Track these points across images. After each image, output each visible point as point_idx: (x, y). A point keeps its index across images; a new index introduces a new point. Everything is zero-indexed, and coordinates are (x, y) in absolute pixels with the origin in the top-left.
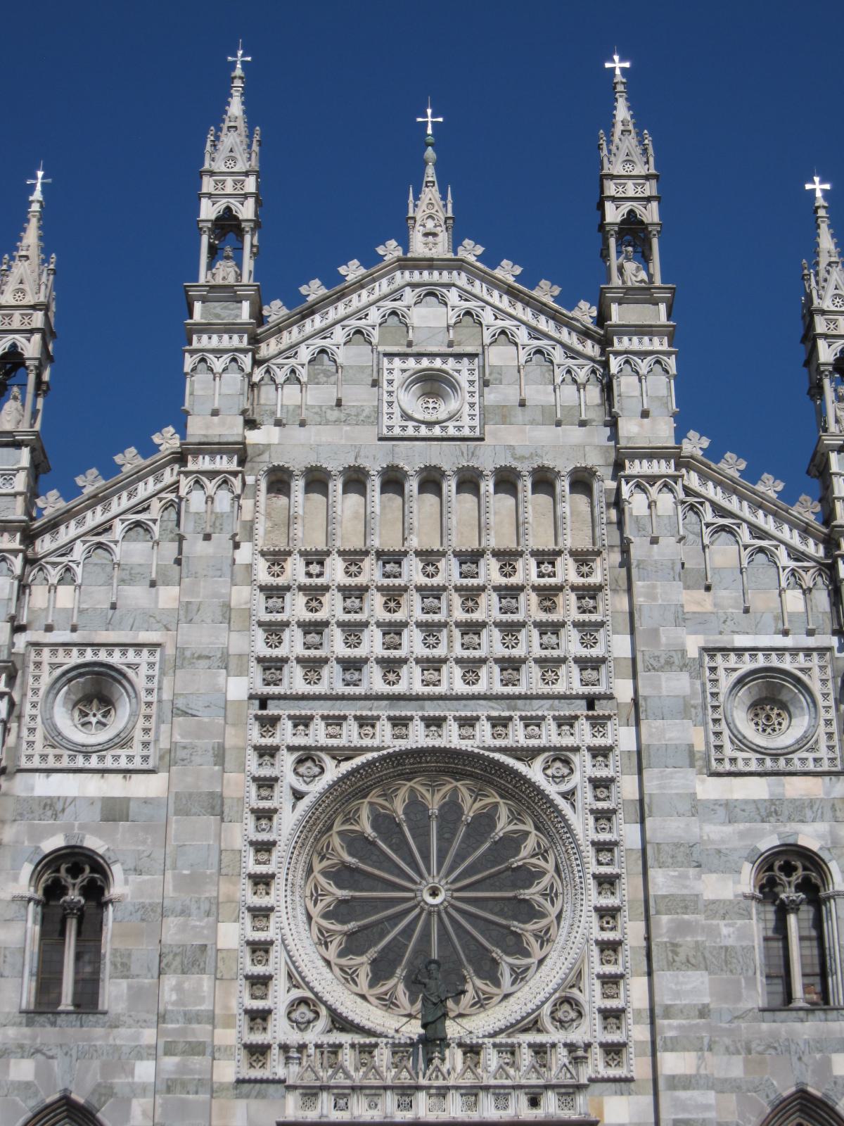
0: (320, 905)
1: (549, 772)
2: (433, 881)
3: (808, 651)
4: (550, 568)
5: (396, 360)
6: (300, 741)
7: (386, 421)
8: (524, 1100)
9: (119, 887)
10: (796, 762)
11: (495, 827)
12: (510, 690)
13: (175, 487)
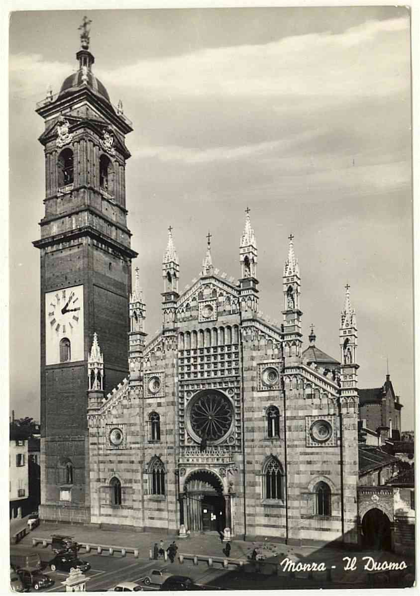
3: (275, 363)
5: (202, 303)
6: (187, 389)
7: (199, 318)
8: (216, 460)
9: (161, 419)
12: (223, 376)
13: (163, 340)
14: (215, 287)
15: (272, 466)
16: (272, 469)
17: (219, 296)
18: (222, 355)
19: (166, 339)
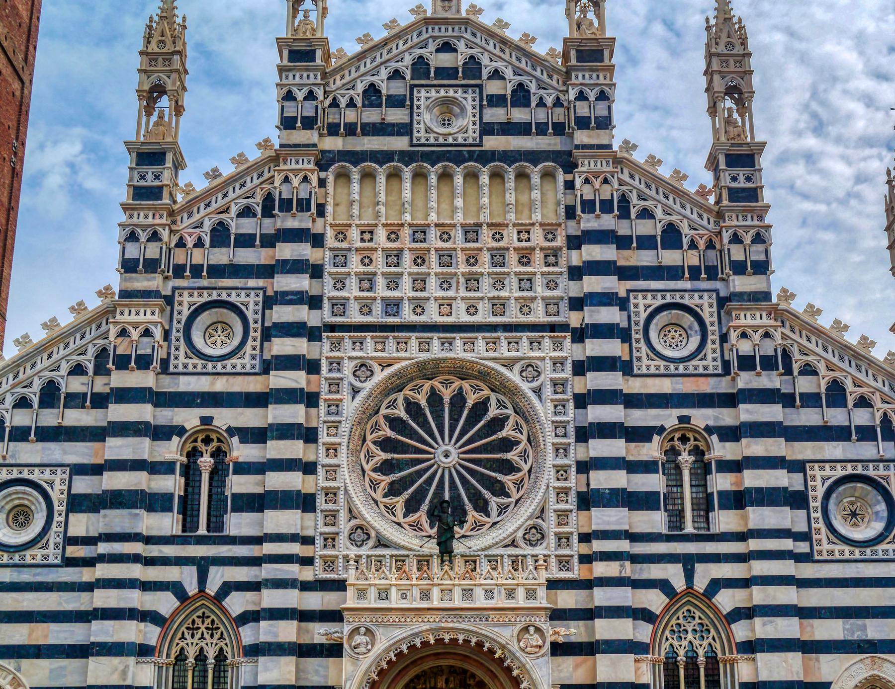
0: (371, 463)
1: (524, 374)
2: (445, 448)
4: (526, 236)
5: (423, 90)
10: (691, 368)
11: (487, 411)
14: (475, 51)
15: (686, 631)
16: (685, 643)
17: (489, 78)
18: (498, 257)
19: (286, 180)
